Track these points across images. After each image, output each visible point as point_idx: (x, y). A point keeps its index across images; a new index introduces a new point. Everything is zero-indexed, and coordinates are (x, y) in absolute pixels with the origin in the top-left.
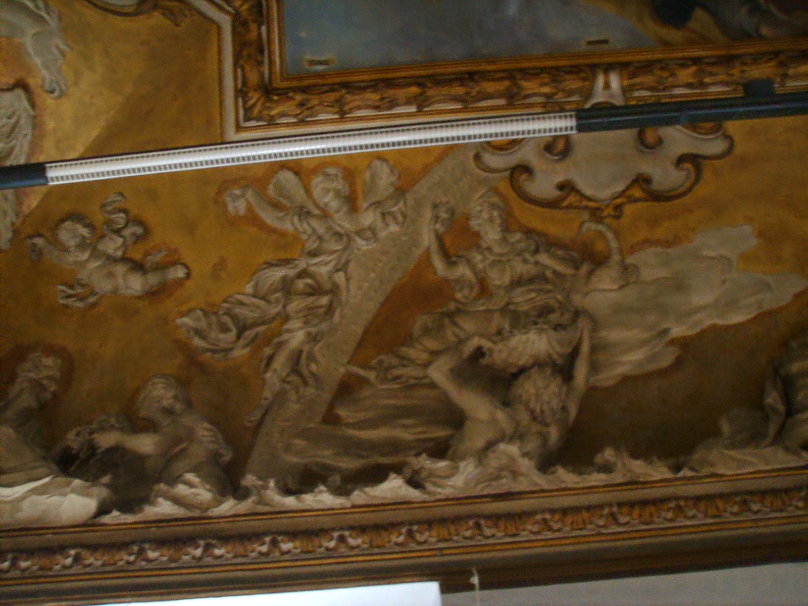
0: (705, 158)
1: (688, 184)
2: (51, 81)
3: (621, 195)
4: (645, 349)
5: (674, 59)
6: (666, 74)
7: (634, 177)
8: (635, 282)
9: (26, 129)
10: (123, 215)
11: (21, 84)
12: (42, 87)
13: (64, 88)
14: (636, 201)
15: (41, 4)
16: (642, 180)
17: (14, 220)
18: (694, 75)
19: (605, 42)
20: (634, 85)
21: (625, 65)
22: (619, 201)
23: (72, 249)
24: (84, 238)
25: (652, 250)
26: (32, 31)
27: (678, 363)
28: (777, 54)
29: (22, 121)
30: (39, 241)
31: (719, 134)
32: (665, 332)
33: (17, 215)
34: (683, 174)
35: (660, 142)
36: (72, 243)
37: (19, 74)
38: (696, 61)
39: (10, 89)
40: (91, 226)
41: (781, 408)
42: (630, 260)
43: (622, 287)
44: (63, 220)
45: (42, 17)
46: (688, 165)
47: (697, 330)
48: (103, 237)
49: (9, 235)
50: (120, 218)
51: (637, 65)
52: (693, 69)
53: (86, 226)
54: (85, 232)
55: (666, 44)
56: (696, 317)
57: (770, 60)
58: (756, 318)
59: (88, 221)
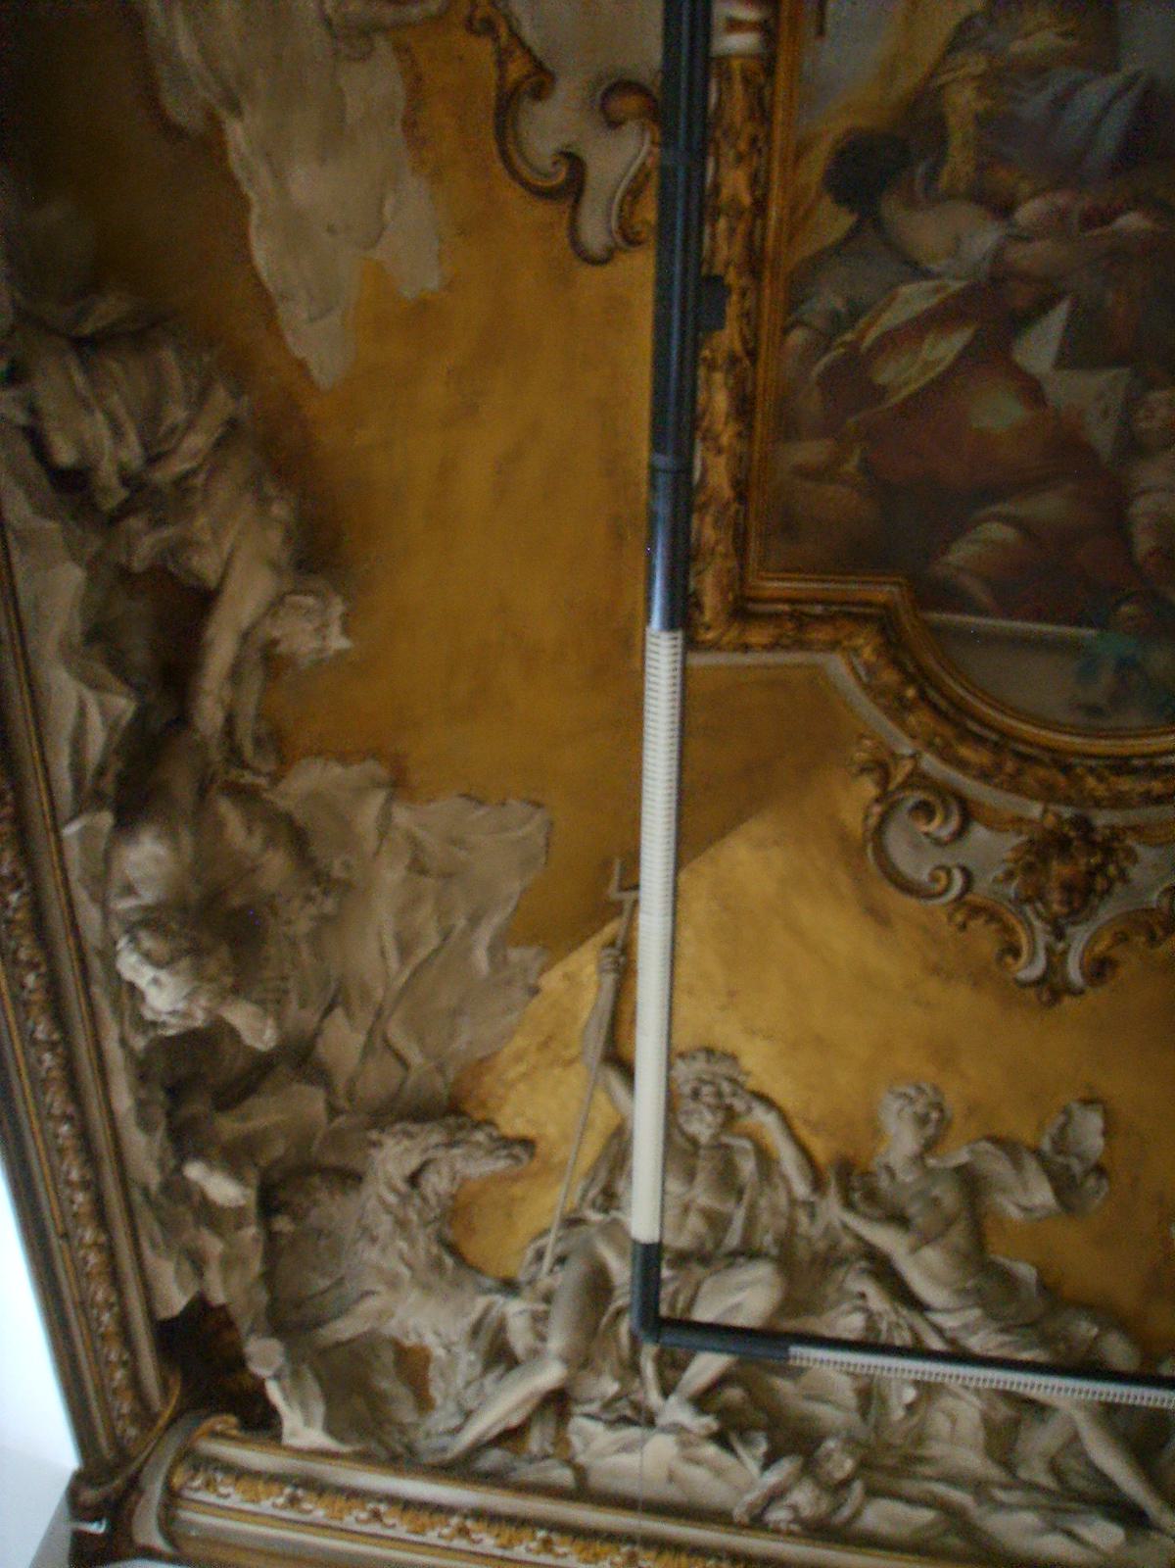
0: (577, 202)
1: (525, 172)
3: (515, 36)
4: (196, 58)
5: (769, 162)
6: (743, 146)
7: (548, 65)
8: (336, 53)
14: (501, 64)
16: (541, 82)
18: (734, 200)
19: (821, 32)
20: (729, 79)
21: (770, 70)
22: (503, 32)
25: (400, 89)
27: (172, 131)
28: (752, 354)
31: (619, 240)
32: (236, 109)
34: (546, 163)
35: (614, 124)
38: (760, 206)
41: (88, 328)
42: (382, 45)
43: (328, 22)
46: (562, 175)
47: (240, 174)
51: (767, 93)
52: (746, 200)
55: (801, 151)
56: (263, 172)
57: (744, 341)
58: (259, 284)
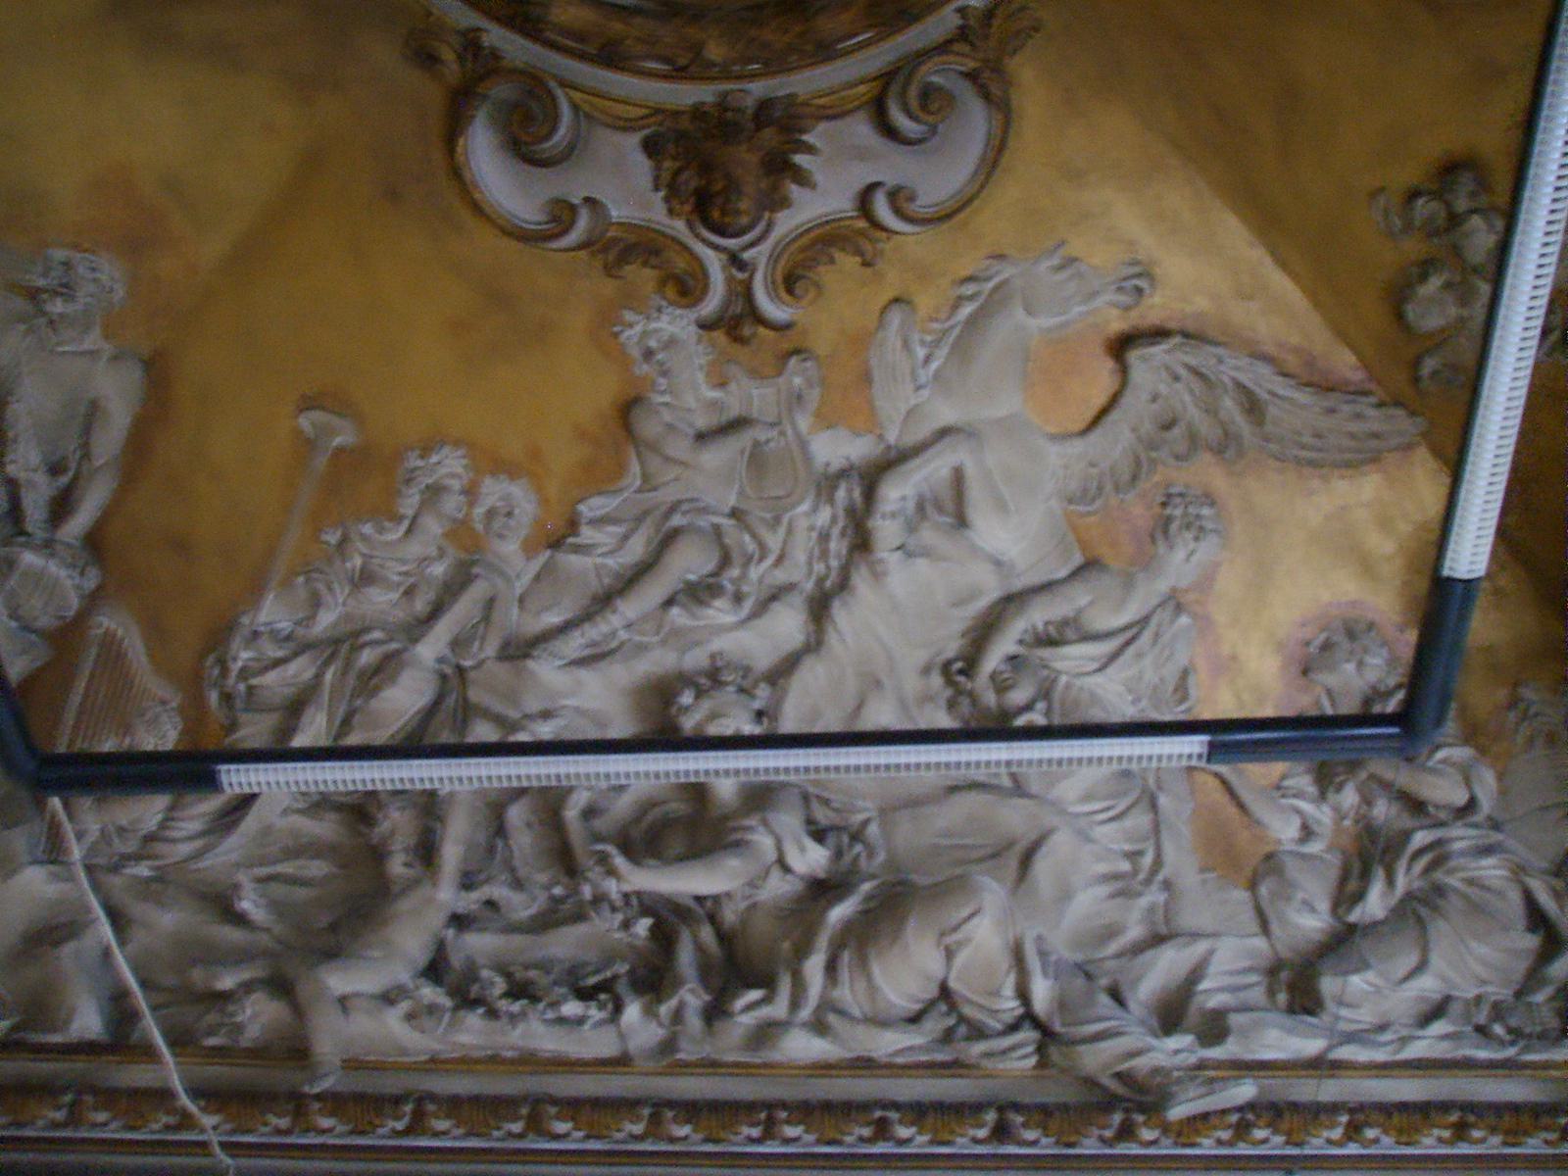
2: (1120, 289)
9: (1202, 357)
10: (1421, 202)
11: (1121, 346)
12: (1127, 308)
13: (1137, 269)
15: (969, 289)
17: (1373, 400)
23: (1465, 313)
24: (1448, 286)
26: (1019, 314)
29: (1193, 361)
30: (1429, 365)
33: (1365, 393)
36: (1453, 311)
37: (1099, 350)
39: (1124, 370)
40: (1426, 267)
44: (1400, 316)
45: (996, 289)
48: (1456, 251)
49: (1400, 412)
50: (1423, 207)
53: (1423, 277)
54: (1434, 283)
59: (1415, 270)
